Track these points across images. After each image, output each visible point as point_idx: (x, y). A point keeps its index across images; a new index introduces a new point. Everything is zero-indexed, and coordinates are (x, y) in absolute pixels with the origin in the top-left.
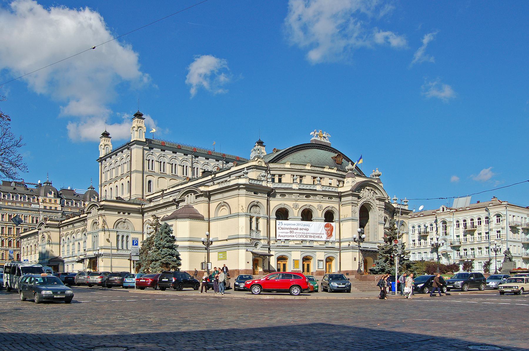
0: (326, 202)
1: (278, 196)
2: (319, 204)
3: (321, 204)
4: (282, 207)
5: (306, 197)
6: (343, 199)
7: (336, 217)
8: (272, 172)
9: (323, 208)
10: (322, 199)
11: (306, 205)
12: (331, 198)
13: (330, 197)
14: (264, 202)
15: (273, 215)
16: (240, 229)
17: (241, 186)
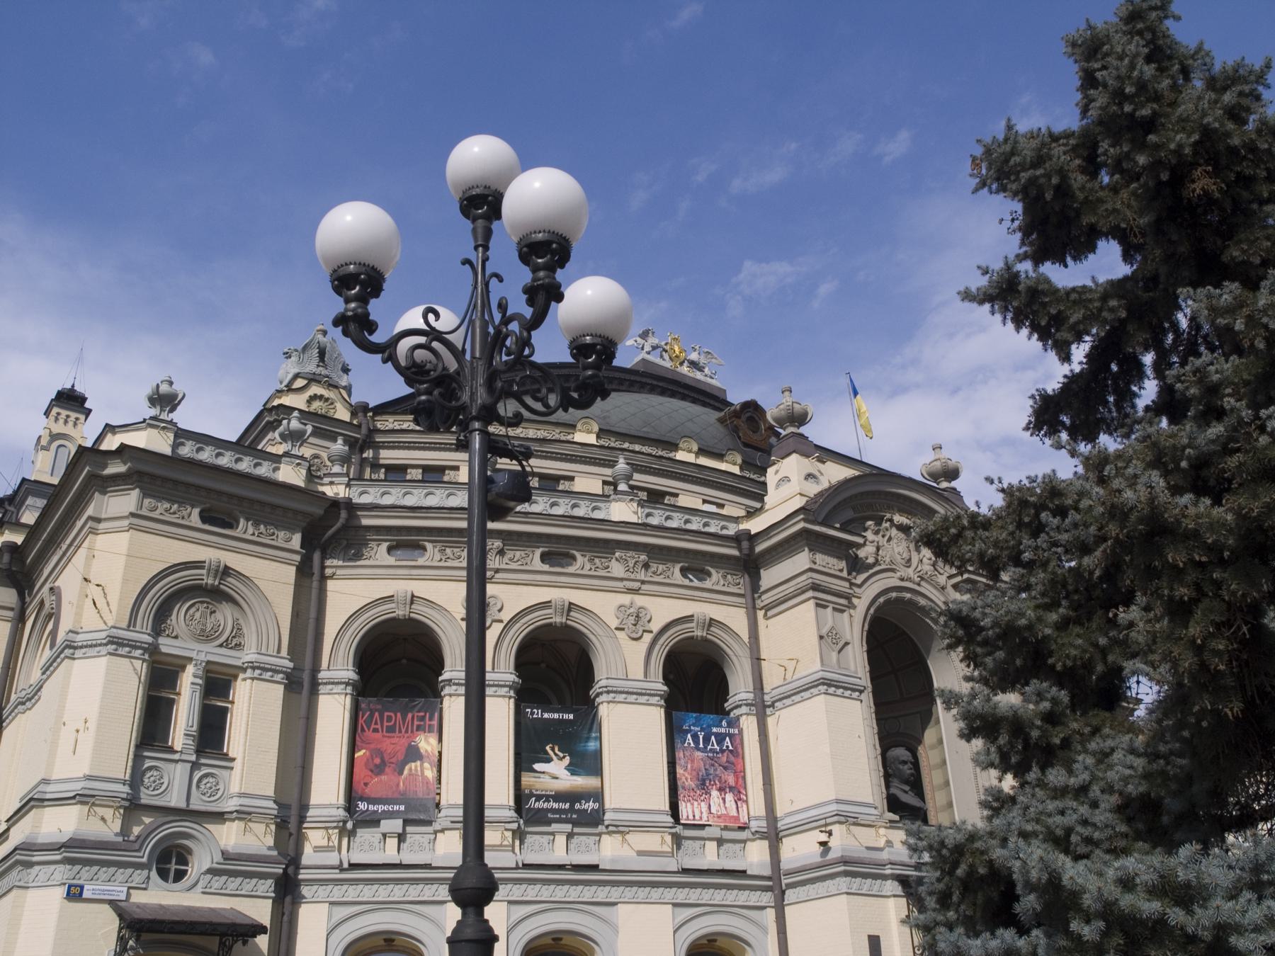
0: (667, 590)
1: (379, 553)
2: (626, 599)
3: (640, 600)
4: (401, 612)
5: (545, 558)
6: (769, 576)
7: (740, 687)
8: (389, 456)
9: (656, 626)
10: (642, 575)
11: (546, 605)
12: (702, 574)
13: (696, 565)
14: (270, 576)
15: (338, 666)
16: (66, 736)
17: (116, 468)
